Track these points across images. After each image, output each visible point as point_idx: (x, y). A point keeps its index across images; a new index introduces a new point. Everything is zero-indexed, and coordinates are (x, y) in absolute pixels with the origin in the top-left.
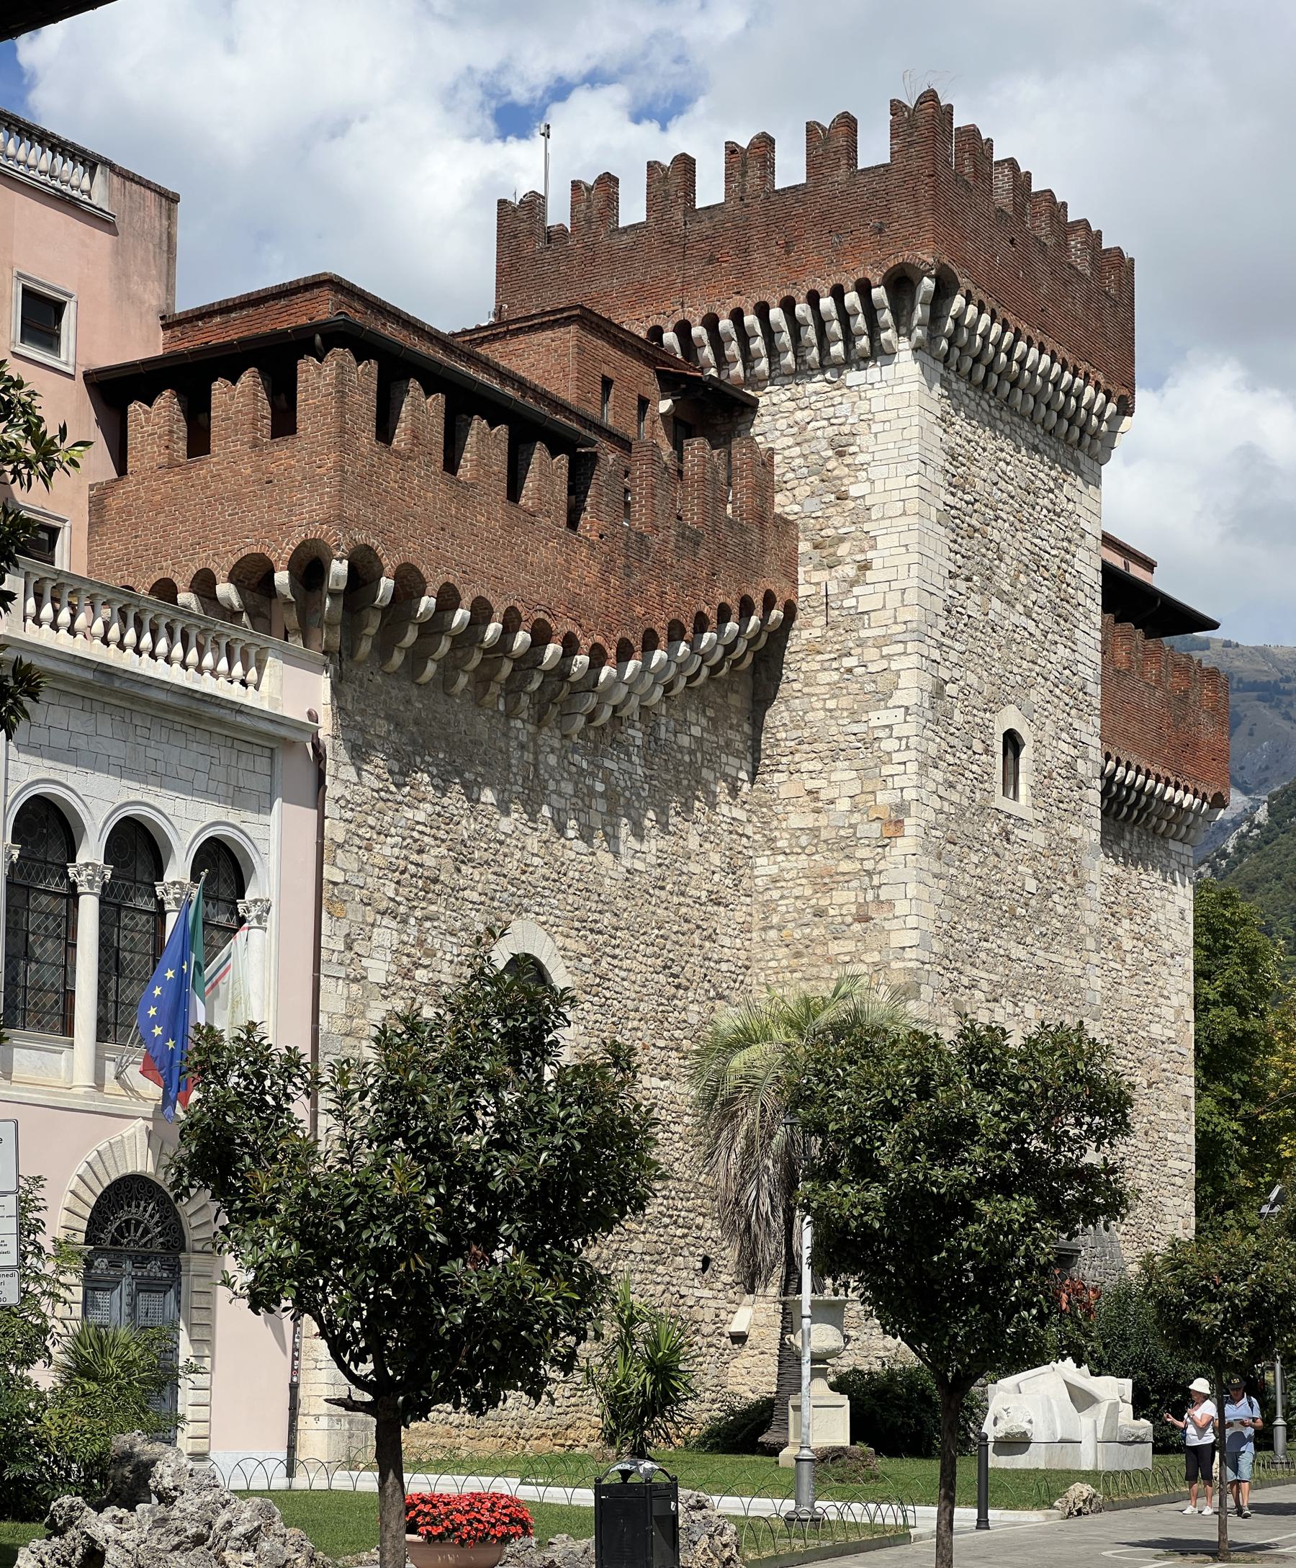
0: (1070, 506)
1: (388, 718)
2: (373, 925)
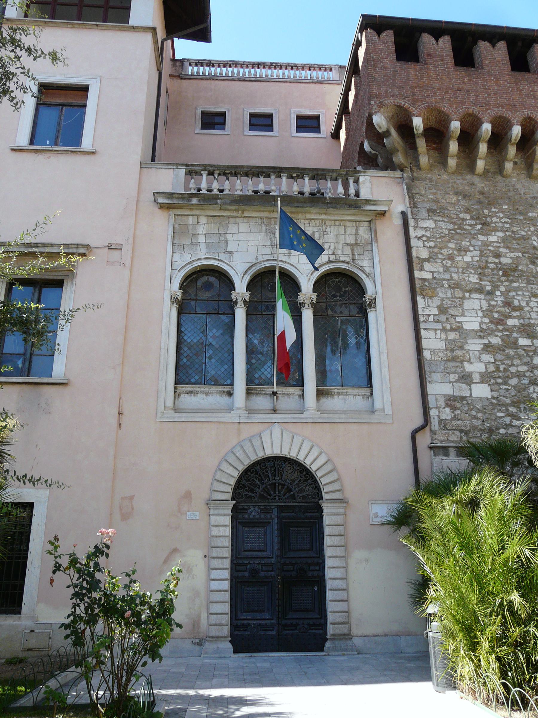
1: (457, 194)
2: (463, 298)
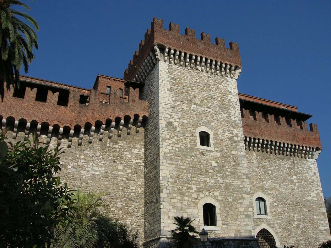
0: (225, 87)
